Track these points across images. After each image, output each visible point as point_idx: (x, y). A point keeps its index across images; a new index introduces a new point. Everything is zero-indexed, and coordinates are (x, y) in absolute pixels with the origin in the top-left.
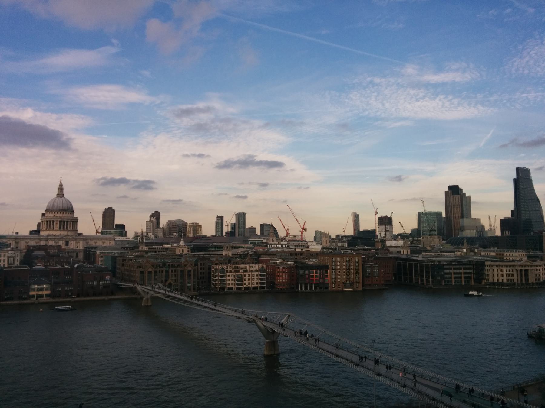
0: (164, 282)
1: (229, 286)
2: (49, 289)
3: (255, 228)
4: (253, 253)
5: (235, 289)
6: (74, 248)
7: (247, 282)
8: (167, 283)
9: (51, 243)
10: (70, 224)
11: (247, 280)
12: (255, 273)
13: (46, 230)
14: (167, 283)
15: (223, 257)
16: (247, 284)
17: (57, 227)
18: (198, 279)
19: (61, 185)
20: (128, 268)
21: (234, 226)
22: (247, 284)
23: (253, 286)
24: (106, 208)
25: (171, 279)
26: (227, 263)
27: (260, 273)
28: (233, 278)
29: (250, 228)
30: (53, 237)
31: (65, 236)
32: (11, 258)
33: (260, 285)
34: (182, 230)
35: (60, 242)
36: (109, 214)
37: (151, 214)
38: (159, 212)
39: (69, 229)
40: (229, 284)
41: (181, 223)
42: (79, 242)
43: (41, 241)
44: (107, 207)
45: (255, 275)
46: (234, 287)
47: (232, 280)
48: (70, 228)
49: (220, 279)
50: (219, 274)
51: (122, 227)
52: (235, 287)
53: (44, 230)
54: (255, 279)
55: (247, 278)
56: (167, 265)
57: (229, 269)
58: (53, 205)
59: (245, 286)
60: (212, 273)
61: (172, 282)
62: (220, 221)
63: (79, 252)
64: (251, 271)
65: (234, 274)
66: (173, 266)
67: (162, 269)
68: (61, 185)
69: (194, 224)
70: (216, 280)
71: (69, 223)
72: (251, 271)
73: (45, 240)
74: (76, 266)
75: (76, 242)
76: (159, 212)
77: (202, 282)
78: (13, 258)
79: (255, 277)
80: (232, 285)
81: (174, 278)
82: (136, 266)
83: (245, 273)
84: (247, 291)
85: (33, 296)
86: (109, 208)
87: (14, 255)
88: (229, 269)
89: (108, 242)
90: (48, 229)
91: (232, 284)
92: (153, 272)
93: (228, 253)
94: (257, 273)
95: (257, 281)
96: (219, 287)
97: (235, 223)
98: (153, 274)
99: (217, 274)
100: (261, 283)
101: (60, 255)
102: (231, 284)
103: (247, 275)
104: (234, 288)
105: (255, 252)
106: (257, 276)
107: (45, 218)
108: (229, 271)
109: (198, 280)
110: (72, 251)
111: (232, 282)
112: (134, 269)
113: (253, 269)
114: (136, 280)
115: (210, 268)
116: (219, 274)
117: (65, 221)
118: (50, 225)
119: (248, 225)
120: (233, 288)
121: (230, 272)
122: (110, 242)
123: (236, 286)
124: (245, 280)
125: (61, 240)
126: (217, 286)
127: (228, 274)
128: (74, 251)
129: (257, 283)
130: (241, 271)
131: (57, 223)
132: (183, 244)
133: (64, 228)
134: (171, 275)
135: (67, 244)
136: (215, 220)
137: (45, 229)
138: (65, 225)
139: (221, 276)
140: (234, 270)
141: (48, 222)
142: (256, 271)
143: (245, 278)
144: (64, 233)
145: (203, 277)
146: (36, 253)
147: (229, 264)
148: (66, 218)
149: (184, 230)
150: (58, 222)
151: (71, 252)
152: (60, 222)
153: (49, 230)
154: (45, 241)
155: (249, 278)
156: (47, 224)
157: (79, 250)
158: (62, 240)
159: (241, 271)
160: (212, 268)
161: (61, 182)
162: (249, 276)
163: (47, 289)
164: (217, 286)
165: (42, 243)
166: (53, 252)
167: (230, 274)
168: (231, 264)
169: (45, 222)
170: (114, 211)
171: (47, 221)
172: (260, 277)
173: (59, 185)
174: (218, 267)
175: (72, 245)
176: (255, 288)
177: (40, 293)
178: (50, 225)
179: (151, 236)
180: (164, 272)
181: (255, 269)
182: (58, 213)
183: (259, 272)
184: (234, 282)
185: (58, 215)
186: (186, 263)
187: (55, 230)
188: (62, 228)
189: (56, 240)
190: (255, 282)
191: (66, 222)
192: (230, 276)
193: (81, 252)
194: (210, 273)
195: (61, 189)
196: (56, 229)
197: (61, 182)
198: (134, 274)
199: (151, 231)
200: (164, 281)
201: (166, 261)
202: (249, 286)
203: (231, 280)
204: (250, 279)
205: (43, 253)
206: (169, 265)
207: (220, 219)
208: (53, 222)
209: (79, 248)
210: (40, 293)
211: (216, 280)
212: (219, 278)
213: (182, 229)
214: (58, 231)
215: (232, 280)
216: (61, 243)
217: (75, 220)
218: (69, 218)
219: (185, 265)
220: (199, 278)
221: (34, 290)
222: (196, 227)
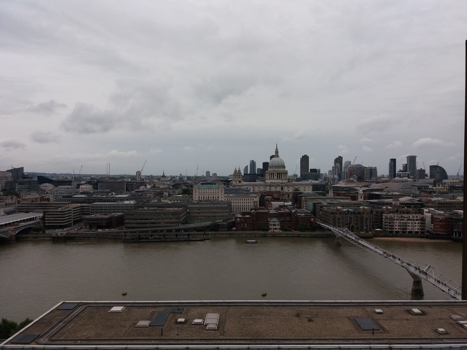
0: (349, 224)
1: (396, 230)
3: (424, 170)
4: (418, 201)
5: (400, 233)
6: (287, 192)
7: (410, 227)
8: (351, 225)
9: (273, 189)
10: (283, 175)
11: (410, 226)
12: (417, 222)
13: (269, 179)
14: (351, 225)
15: (392, 206)
16: (410, 229)
17: (275, 177)
18: (373, 222)
19: (277, 149)
20: (324, 213)
21: (405, 167)
22: (410, 229)
23: (415, 231)
25: (354, 223)
26: (395, 213)
27: (421, 222)
28: (399, 224)
29: (419, 170)
30: (274, 184)
31: (281, 184)
33: (421, 231)
34: (360, 173)
35: (278, 187)
36: (305, 160)
37: (336, 159)
39: (283, 179)
40: (396, 229)
41: (360, 167)
42: (289, 188)
43: (267, 186)
44: (303, 155)
45: (417, 223)
46: (400, 230)
47: (399, 226)
48: (283, 178)
50: (389, 221)
51: (314, 171)
52: (401, 231)
53: (268, 179)
54: (417, 226)
55: (410, 225)
56: (351, 213)
57: (396, 218)
58: (273, 163)
59: (409, 230)
60: (383, 220)
61: (354, 225)
62: (393, 163)
63: (290, 194)
64: (414, 220)
65: (400, 221)
66: (354, 213)
67: (347, 215)
68: (277, 149)
69: (370, 168)
70: (386, 225)
71: (283, 174)
72: (414, 220)
73: (269, 186)
74: (293, 211)
75: (287, 188)
77: (376, 225)
79: (417, 225)
80: (398, 229)
81: (355, 222)
82: (330, 213)
83: (408, 221)
84: (410, 235)
85: (271, 228)
86: (305, 155)
88: (396, 218)
89: (308, 187)
90: (270, 179)
91: (399, 229)
92: (341, 218)
93: (397, 203)
94: (419, 222)
95: (419, 228)
96: (389, 230)
97: (406, 164)
98: (341, 219)
99: (386, 221)
100: (421, 229)
101: (280, 198)
102: (397, 229)
103: (410, 223)
104: (400, 231)
105: (419, 201)
106: (418, 224)
107: (268, 171)
108: (396, 220)
109: (373, 224)
110: (285, 193)
111: (399, 227)
112: (329, 215)
113: (415, 218)
114: (330, 222)
115: (382, 216)
116: (389, 221)
117: (280, 173)
118: (271, 176)
119: (419, 167)
120: (399, 231)
121: (397, 220)
122: (309, 187)
123: (402, 230)
124: (408, 226)
125: (278, 186)
126: (387, 230)
127: (395, 221)
128: (287, 193)
129: (418, 229)
130: (405, 219)
134: (354, 220)
135: (282, 189)
136: (389, 162)
137: (268, 179)
138: (280, 176)
139: (390, 223)
140: (400, 218)
141: (270, 174)
142: (417, 220)
143: (408, 225)
144: (280, 181)
145: (377, 221)
146: (266, 197)
147: (396, 214)
148: (281, 171)
149: (362, 172)
151: (285, 194)
152: (277, 174)
153: (271, 179)
154: (269, 186)
155: (412, 224)
156: (270, 176)
157: (290, 192)
158: (279, 186)
159: (405, 219)
161: (277, 147)
162: (412, 224)
164: (387, 230)
165: (268, 189)
166: (276, 196)
167: (397, 221)
168: (397, 214)
169: (269, 174)
170: (308, 157)
171: (270, 174)
172: (421, 225)
173: (276, 149)
174: (388, 216)
175: (285, 189)
176: (417, 232)
177: (275, 227)
178: (271, 176)
179: (336, 177)
180: (349, 218)
181: (417, 218)
182: (276, 168)
183: (420, 221)
184: (400, 228)
185: (275, 170)
186: (364, 212)
187: (275, 179)
188: (279, 178)
189: (275, 186)
190: (417, 228)
192: (397, 223)
193: (291, 194)
194: (382, 219)
195: (277, 152)
196: (275, 179)
197: (277, 147)
198: (329, 218)
199: (337, 174)
200: (349, 223)
201: (350, 210)
202: (412, 230)
203: (397, 226)
204: (413, 226)
205: (270, 197)
206: (352, 213)
207: (393, 161)
208: (273, 174)
209: (289, 192)
210: (275, 227)
211: (386, 225)
212: (389, 224)
213: (361, 171)
215: (399, 226)
217: (286, 173)
218: (283, 171)
219: (364, 214)
220: (374, 222)
221: (271, 225)
222: (372, 171)
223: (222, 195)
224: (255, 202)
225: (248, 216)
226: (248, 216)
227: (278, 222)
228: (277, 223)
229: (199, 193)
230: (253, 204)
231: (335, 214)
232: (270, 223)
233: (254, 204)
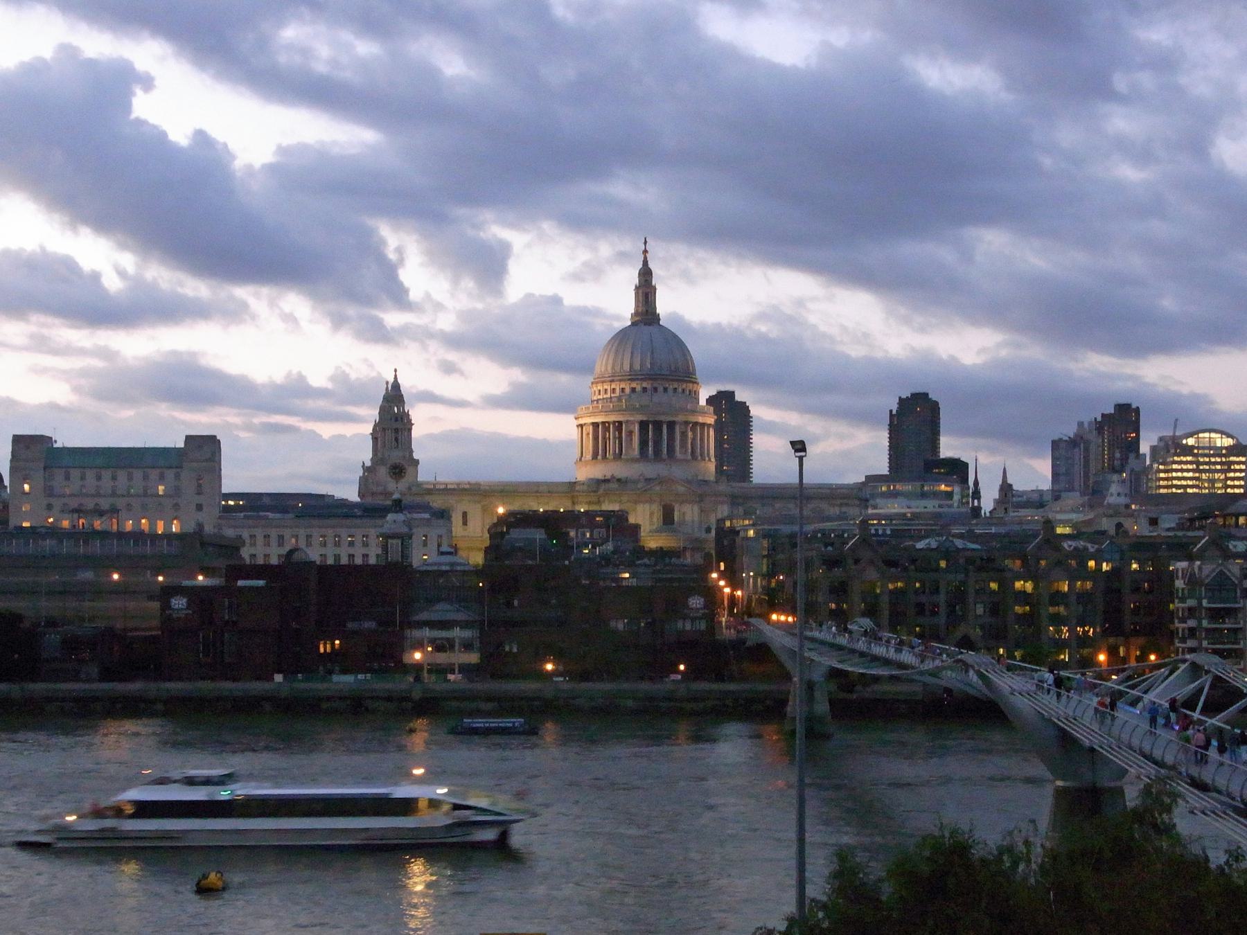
2: (477, 644)
6: (697, 535)
19: (646, 274)
24: (904, 396)
32: (394, 541)
37: (1099, 419)
38: (1134, 406)
39: (678, 454)
44: (906, 394)
49: (1207, 630)
76: (1134, 406)
78: (398, 542)
87: (405, 530)
90: (599, 457)
131: (630, 433)
132: (1123, 500)
133: (657, 452)
139: (1215, 615)
146: (517, 534)
150: (636, 428)
152: (643, 425)
156: (596, 438)
160: (1178, 578)
163: (467, 646)
170: (934, 408)
171: (595, 425)
191: (665, 427)
205: (539, 535)
212: (1205, 623)
214: (636, 466)
216: (644, 516)
223: (199, 507)
224: (387, 537)
225: (261, 583)
226: (261, 583)
227: (465, 625)
228: (467, 634)
229: (51, 495)
230: (379, 551)
231: (850, 561)
232: (408, 633)
233: (385, 548)
